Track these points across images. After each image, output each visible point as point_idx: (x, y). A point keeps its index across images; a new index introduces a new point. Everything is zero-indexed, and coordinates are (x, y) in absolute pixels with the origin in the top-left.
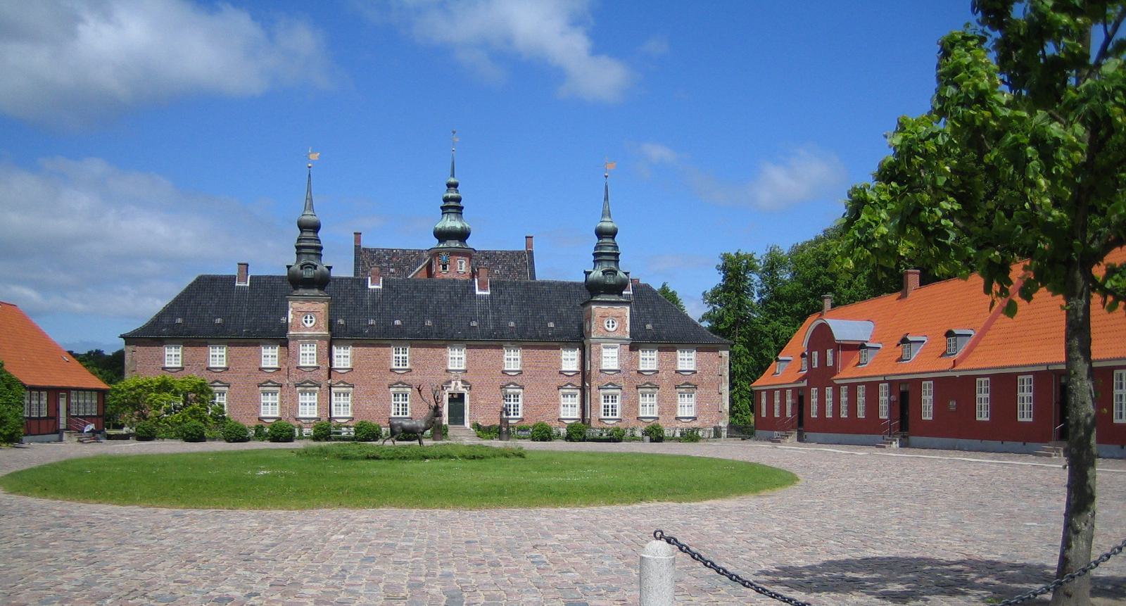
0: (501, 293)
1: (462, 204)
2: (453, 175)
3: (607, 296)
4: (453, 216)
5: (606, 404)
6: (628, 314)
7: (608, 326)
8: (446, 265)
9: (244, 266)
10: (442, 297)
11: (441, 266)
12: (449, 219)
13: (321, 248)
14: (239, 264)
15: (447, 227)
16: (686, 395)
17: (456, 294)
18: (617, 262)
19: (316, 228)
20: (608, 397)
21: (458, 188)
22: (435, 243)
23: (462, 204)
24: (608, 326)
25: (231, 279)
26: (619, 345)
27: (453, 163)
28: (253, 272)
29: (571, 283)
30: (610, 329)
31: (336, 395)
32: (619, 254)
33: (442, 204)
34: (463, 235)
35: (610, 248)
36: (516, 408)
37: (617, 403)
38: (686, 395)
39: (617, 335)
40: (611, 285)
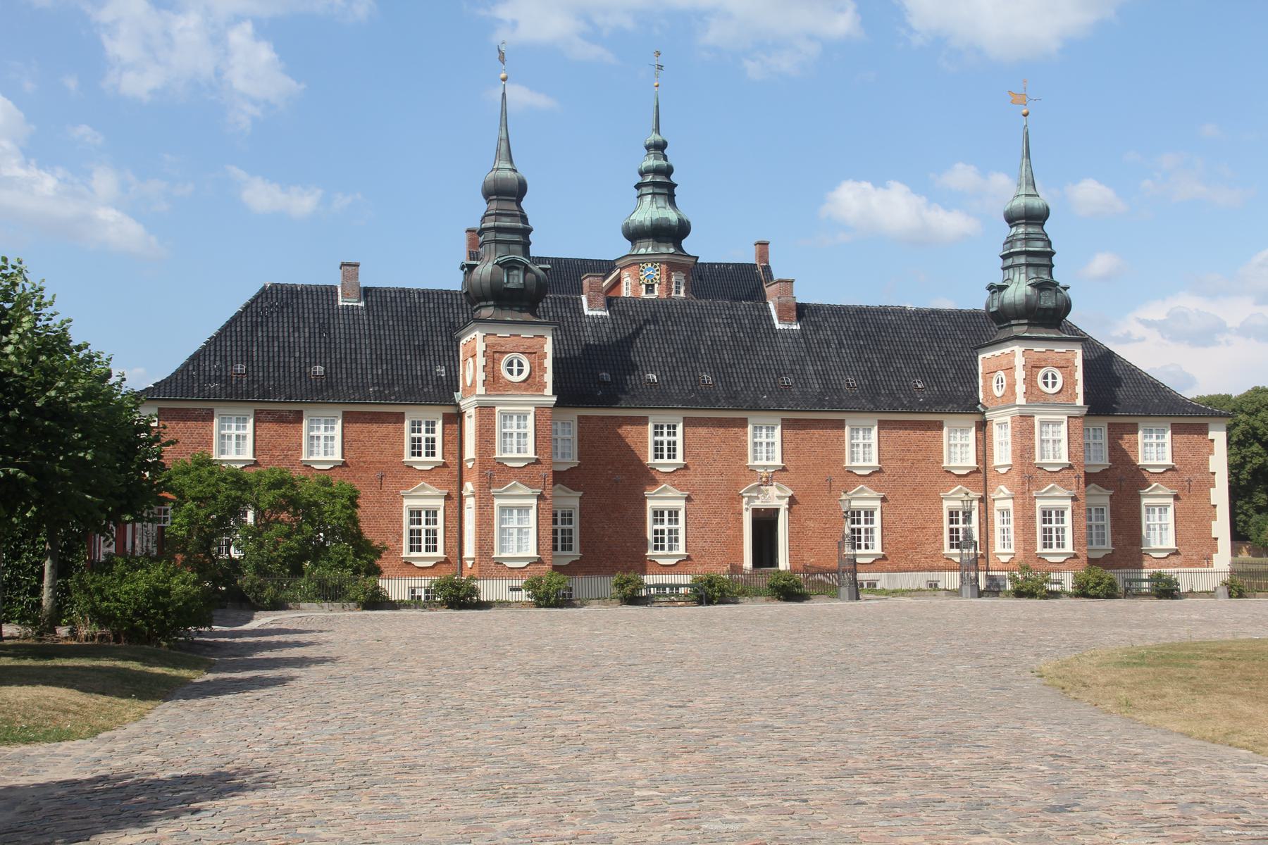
0: (818, 328)
1: (674, 178)
2: (657, 130)
3: (1042, 330)
4: (661, 201)
5: (567, 526)
6: (1079, 362)
7: (1046, 384)
8: (653, 286)
9: (350, 268)
10: (718, 332)
11: (644, 286)
12: (654, 205)
13: (529, 231)
14: (343, 265)
15: (654, 218)
16: (1157, 509)
17: (741, 326)
18: (1050, 267)
19: (518, 191)
20: (1050, 514)
21: (666, 151)
22: (619, 248)
23: (674, 178)
24: (1046, 384)
25: (330, 292)
26: (1065, 418)
27: (657, 107)
28: (366, 280)
29: (933, 312)
30: (1050, 390)
31: (1148, 511)
32: (1054, 253)
33: (639, 179)
34: (674, 233)
35: (1040, 244)
36: (1060, 534)
37: (1105, 522)
38: (1157, 509)
39: (1061, 399)
40: (1047, 309)
